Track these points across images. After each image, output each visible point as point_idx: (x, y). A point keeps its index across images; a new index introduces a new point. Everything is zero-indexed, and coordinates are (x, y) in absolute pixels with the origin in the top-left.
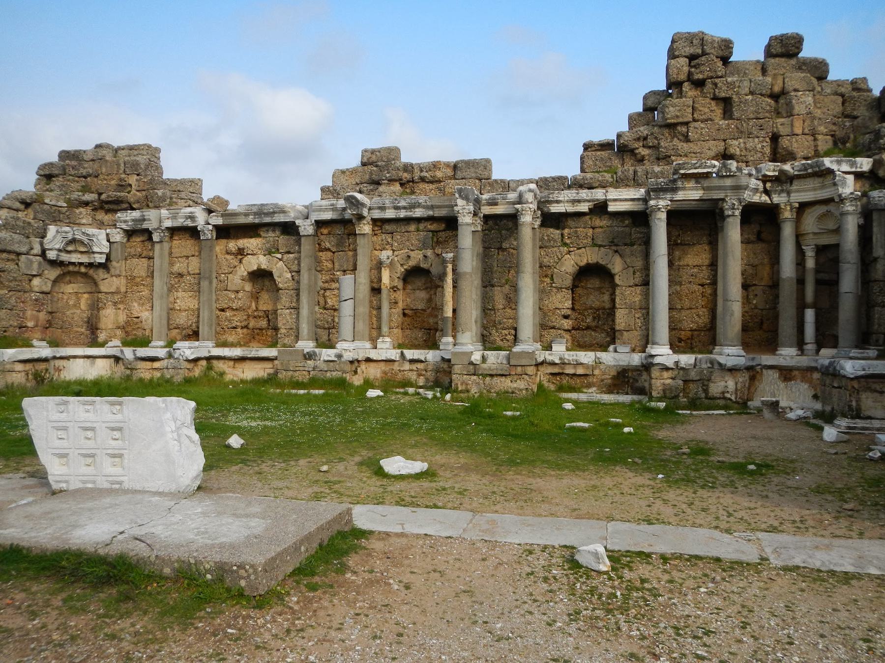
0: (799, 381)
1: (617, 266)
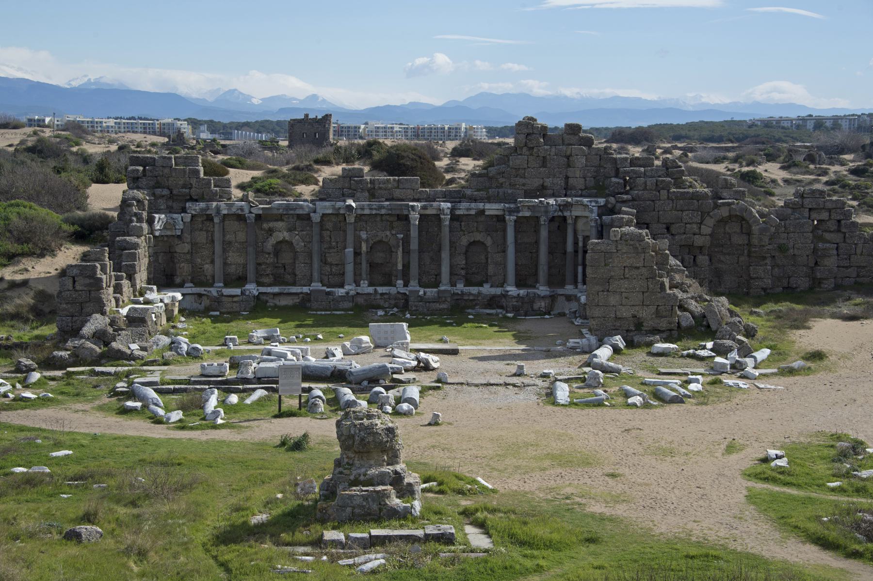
1: (489, 242)
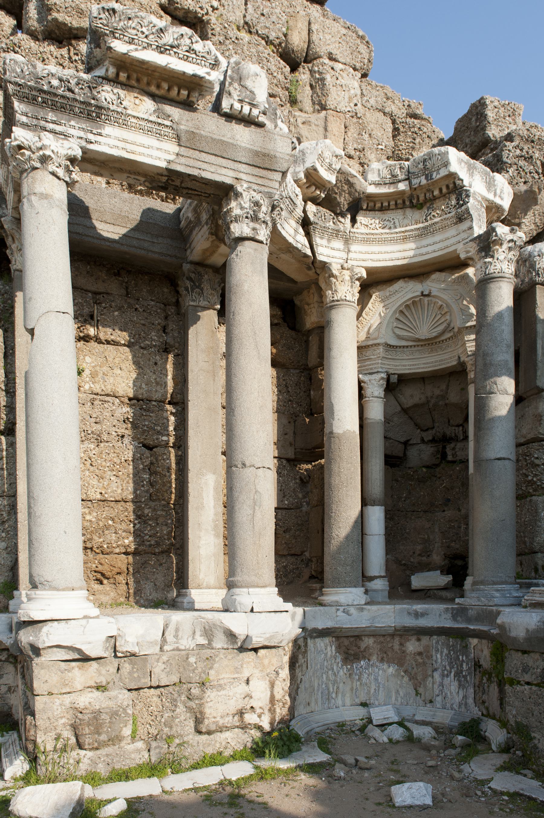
0: (374, 658)
